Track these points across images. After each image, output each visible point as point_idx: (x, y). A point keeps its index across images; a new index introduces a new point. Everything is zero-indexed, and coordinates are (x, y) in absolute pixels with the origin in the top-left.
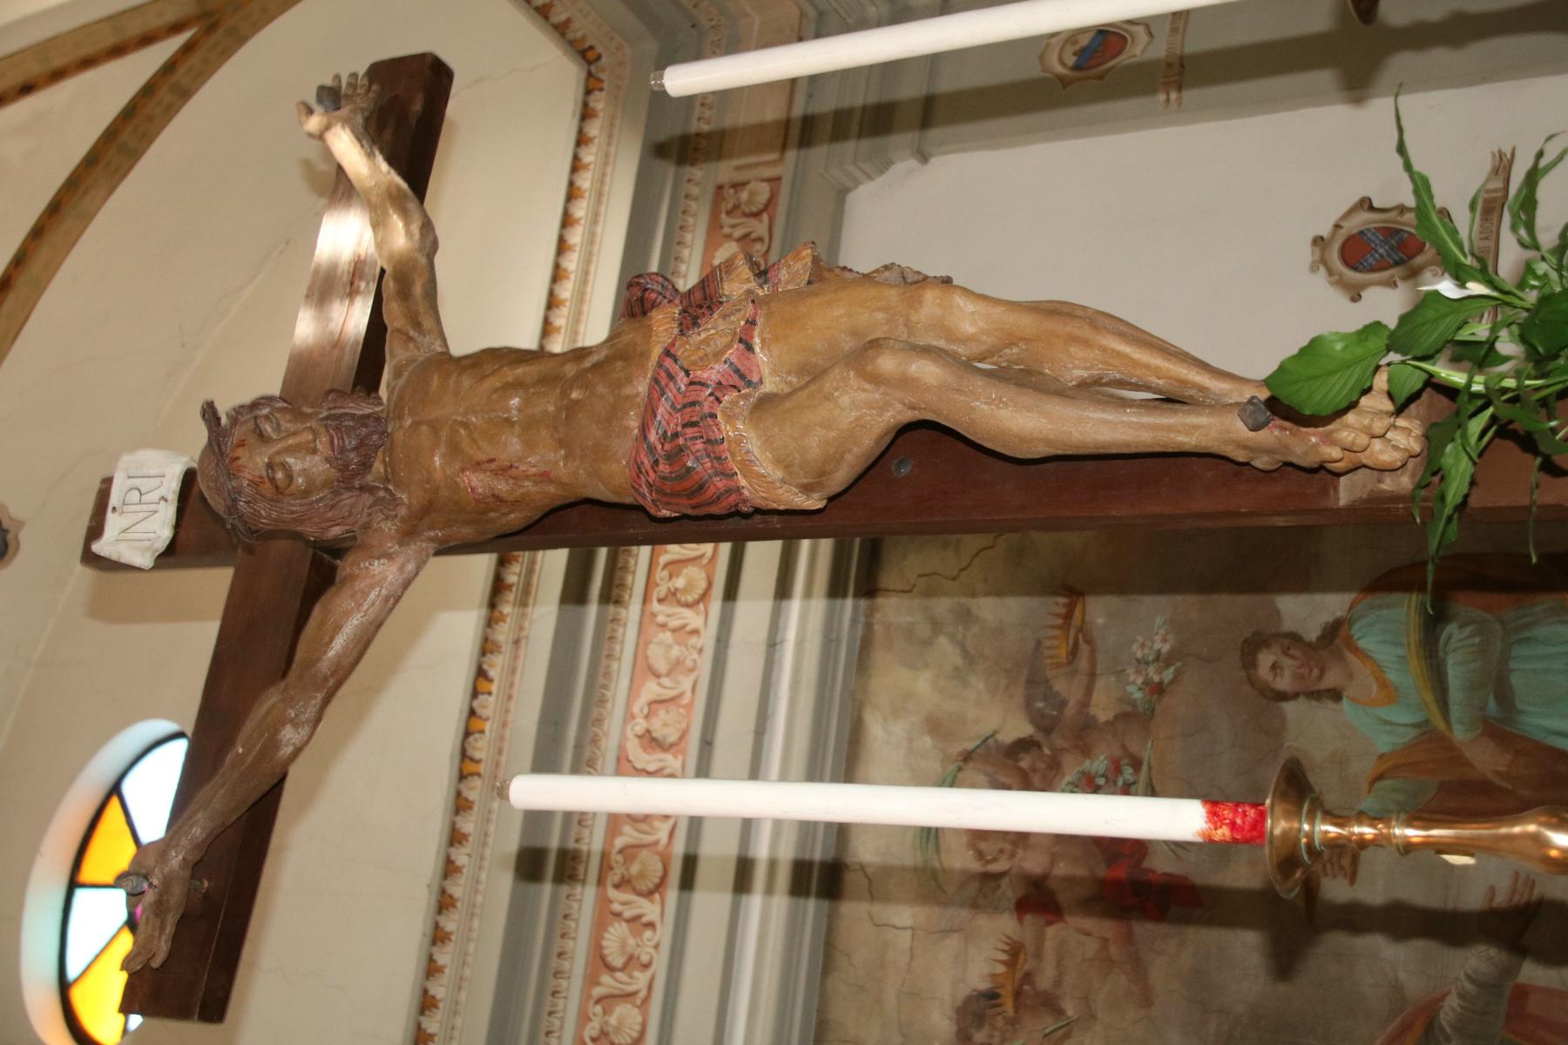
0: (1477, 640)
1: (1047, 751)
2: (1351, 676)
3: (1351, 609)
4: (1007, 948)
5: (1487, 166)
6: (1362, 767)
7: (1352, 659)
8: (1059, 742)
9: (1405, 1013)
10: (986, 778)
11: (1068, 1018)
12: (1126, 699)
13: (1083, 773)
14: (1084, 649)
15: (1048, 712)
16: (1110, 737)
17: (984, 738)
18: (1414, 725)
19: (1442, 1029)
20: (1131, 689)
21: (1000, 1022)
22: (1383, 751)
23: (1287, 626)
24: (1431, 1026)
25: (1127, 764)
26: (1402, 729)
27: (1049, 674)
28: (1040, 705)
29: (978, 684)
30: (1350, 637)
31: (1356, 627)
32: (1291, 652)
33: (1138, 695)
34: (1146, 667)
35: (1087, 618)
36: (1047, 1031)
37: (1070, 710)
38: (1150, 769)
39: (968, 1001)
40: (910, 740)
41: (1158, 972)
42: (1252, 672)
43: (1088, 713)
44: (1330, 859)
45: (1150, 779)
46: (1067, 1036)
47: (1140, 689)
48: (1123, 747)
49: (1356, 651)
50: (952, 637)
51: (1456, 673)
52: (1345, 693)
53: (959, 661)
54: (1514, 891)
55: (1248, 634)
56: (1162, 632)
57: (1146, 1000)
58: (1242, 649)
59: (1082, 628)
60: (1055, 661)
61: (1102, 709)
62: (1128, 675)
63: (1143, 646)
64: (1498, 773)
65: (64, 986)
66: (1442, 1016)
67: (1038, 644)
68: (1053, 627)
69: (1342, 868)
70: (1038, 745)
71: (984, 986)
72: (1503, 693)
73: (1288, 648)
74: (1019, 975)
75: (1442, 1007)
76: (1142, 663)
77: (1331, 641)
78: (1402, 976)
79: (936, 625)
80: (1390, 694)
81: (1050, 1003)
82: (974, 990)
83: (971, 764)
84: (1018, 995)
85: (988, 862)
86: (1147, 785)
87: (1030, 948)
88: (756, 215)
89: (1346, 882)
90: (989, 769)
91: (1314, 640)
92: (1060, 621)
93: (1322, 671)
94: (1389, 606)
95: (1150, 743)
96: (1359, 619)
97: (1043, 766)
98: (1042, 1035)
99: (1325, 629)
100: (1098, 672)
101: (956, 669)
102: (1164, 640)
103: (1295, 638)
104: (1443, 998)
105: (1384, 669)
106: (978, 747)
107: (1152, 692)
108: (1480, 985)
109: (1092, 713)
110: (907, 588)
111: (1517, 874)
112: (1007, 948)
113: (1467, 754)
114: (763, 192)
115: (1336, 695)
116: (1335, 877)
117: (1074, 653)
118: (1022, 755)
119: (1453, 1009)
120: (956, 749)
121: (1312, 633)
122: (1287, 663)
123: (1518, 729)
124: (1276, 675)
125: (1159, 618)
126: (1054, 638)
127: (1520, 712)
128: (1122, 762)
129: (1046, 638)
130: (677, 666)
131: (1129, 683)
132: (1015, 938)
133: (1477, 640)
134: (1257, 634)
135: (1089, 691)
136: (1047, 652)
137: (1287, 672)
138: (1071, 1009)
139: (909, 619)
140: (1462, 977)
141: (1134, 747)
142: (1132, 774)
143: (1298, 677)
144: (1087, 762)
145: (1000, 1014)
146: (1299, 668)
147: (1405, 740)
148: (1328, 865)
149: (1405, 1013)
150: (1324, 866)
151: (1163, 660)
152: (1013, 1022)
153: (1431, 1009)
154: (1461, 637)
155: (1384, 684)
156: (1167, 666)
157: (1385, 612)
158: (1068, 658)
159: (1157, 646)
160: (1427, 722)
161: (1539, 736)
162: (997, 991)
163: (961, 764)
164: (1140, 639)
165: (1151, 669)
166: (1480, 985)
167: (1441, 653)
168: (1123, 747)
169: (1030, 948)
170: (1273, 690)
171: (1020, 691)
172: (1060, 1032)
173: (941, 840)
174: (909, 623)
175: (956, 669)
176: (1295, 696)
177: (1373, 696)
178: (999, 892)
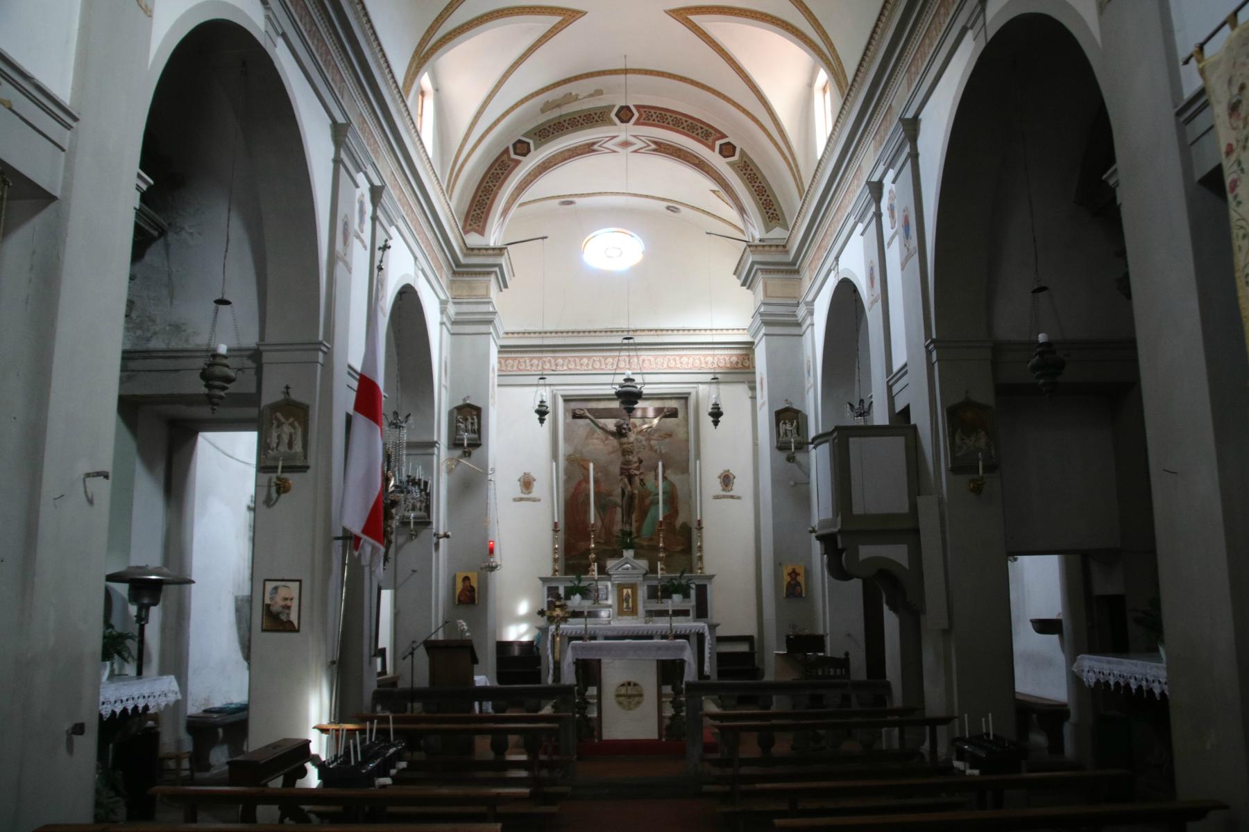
5: (739, 495)
41: (613, 455)
65: (594, 237)
76: (660, 448)
88: (742, 364)
114: (746, 365)
130: (656, 364)
138: (606, 442)
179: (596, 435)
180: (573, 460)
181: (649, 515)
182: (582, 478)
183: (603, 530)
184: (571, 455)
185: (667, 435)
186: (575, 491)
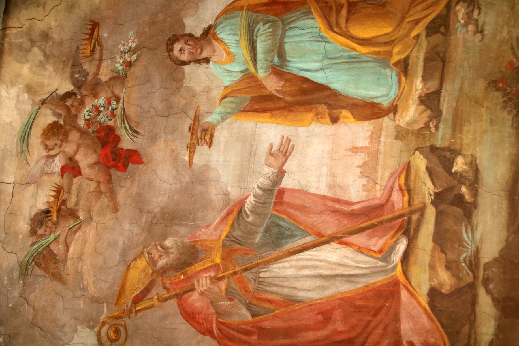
0: (271, 30)
1: (79, 97)
2: (214, 51)
3: (216, 20)
4: (56, 189)
6: (217, 93)
7: (215, 43)
8: (84, 92)
9: (230, 206)
10: (50, 111)
11: (81, 220)
12: (115, 71)
13: (94, 106)
14: (98, 48)
15: (80, 79)
16: (107, 88)
17: (51, 93)
18: (241, 72)
19: (245, 212)
20: (117, 65)
21: (50, 224)
22: (226, 85)
23: (188, 31)
24: (240, 212)
25: (114, 100)
26: (237, 74)
27: (82, 61)
28: (77, 76)
29: (50, 68)
30: (215, 33)
31: (218, 28)
32: (189, 42)
33: (120, 68)
34: (124, 54)
35: (100, 35)
36: (71, 227)
37: (90, 77)
38: (123, 101)
39: (37, 215)
40: (18, 96)
41: (122, 196)
42: (171, 53)
43: (98, 78)
44: (201, 136)
45: (124, 106)
46: (79, 228)
47: (121, 65)
48: (113, 92)
49: (217, 39)
50: (39, 47)
51: (261, 46)
52: (211, 59)
53: (42, 58)
54: (281, 145)
55: (170, 36)
56: (132, 38)
57: (115, 209)
58: (167, 42)
59: (98, 39)
60: (84, 55)
61: (104, 77)
62: (117, 59)
63: (124, 45)
64: (278, 91)
66: (246, 206)
67: (78, 48)
68: (84, 39)
69: (206, 141)
70: (75, 94)
71: (44, 207)
72: (281, 54)
73: (188, 41)
74: (60, 201)
75: (246, 202)
77: (206, 37)
78: (229, 189)
79: (33, 42)
80: (231, 57)
81: (73, 214)
82: (39, 210)
83: (45, 105)
84: (59, 211)
85: (50, 150)
86: (122, 109)
87: (66, 189)
89: (208, 147)
90: (53, 107)
91: (199, 36)
92: (88, 37)
93: (202, 50)
94: (233, 18)
95: (124, 90)
96: (219, 24)
97: (77, 104)
98: (68, 228)
99: (204, 31)
100: (103, 59)
101: (41, 62)
102: (133, 42)
103: (191, 36)
104: (246, 198)
105: (229, 47)
106: (48, 97)
107: (126, 66)
108: (264, 190)
109: (99, 78)
110: (20, 26)
111: (283, 137)
112: (56, 189)
113: (264, 84)
115: (207, 60)
116: (202, 145)
117: (93, 51)
118: (68, 99)
119: (251, 202)
120: (38, 99)
121: (198, 33)
122: (187, 48)
123: (287, 69)
124: (181, 53)
125: (131, 32)
126: (85, 44)
127: (289, 61)
128: (111, 100)
129: (82, 45)
131: (117, 63)
132: (59, 185)
133: (271, 30)
134: (175, 35)
135: (99, 67)
136: (81, 51)
137: (186, 52)
138: (82, 215)
139: (21, 40)
140: (256, 187)
141: (117, 92)
142: (115, 105)
143: (191, 53)
144: (96, 100)
145: (50, 220)
146: (192, 50)
147: (237, 79)
148: (200, 140)
149: (230, 206)
150: (198, 141)
151: (132, 51)
152: (56, 224)
153: (241, 203)
154: (264, 29)
155: (229, 54)
156: (134, 54)
157: (231, 21)
158: (90, 53)
159: (130, 45)
160: (247, 69)
161: (296, 72)
162: (49, 209)
163: (40, 105)
164: (123, 42)
165: (127, 56)
166: (264, 190)
167: (255, 38)
168: (113, 92)
169: (66, 189)
170: (180, 61)
171: (68, 70)
172: (76, 227)
173: (29, 142)
174: (20, 42)
175: (41, 62)
176: (189, 62)
177: (224, 59)
178: (54, 164)
179: (58, 249)
180: (117, 331)
181: (319, 78)
182: (173, 304)
183: (359, 239)
184: (99, 334)
185: (91, 34)
186: (209, 332)
